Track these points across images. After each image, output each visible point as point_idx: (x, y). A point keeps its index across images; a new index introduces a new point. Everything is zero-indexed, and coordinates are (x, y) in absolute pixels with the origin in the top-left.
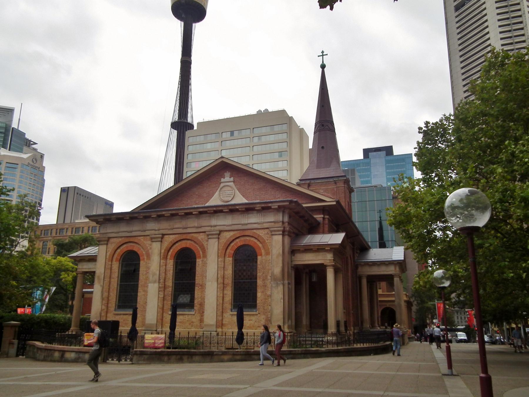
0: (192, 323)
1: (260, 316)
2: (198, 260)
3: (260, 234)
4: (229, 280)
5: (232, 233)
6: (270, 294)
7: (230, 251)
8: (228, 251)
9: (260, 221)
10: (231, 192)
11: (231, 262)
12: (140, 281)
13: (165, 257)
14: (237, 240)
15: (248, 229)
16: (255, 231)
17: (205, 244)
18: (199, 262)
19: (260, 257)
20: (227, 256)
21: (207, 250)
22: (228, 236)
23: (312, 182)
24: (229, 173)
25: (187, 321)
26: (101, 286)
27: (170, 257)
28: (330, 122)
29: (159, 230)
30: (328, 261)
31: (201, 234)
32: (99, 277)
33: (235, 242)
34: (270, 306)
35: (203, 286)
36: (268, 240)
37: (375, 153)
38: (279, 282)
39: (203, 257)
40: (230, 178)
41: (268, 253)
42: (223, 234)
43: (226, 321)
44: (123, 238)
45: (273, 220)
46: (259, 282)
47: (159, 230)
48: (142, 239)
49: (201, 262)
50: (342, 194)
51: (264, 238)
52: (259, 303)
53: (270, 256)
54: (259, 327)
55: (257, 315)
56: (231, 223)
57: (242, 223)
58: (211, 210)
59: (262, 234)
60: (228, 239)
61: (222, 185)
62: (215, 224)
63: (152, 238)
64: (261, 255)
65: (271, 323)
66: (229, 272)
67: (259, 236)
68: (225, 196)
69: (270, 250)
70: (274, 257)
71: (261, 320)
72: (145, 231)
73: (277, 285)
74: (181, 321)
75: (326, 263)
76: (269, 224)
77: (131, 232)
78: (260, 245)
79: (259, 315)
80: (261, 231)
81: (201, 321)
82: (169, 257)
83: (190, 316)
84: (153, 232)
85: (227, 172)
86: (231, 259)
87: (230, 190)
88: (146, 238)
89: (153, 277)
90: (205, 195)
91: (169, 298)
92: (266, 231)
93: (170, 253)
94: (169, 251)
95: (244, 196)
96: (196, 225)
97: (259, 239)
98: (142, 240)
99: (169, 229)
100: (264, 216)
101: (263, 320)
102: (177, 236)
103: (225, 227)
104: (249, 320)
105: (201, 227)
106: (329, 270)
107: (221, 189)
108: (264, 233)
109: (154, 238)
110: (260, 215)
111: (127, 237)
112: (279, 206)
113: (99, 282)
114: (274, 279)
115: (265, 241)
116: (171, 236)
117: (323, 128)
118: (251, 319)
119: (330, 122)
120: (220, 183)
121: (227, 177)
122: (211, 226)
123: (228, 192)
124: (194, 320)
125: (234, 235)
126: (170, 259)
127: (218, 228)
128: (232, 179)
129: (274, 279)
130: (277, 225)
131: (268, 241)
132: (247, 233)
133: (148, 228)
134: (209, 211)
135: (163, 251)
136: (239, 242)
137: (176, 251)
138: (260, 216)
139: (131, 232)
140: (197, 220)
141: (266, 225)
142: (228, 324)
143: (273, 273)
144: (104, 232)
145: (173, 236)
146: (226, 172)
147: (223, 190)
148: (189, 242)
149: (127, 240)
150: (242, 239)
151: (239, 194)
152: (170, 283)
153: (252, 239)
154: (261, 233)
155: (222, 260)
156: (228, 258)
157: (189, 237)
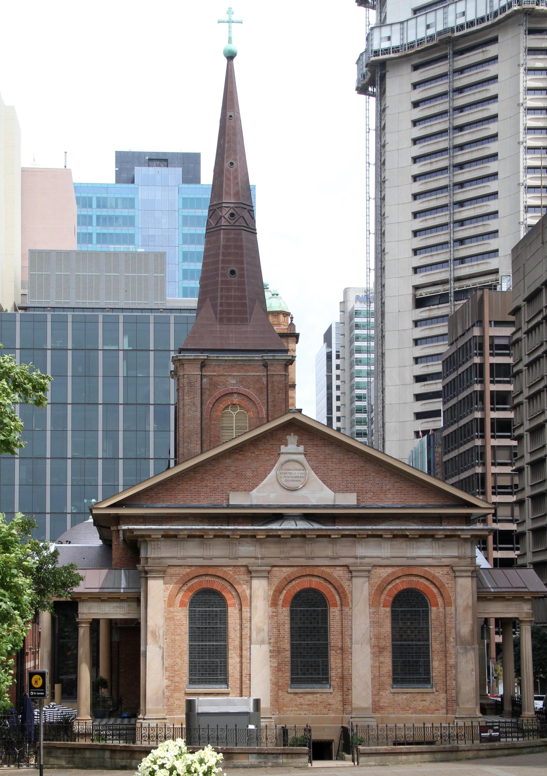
0: (329, 706)
1: (437, 695)
2: (332, 609)
3: (436, 574)
4: (388, 643)
5: (390, 570)
6: (454, 663)
7: (387, 597)
8: (383, 597)
9: (437, 554)
10: (300, 472)
11: (389, 614)
12: (230, 641)
13: (274, 603)
14: (398, 581)
15: (416, 566)
16: (427, 568)
17: (345, 584)
18: (334, 613)
19: (436, 608)
20: (382, 605)
21: (349, 595)
22: (384, 573)
23: (213, 356)
24: (296, 438)
25: (321, 702)
26: (160, 647)
27: (283, 602)
28: (249, 208)
29: (262, 558)
30: (524, 615)
31: (338, 568)
32: (154, 633)
33: (394, 584)
34: (454, 680)
35: (344, 651)
36: (448, 584)
37: (152, 170)
38: (468, 647)
39: (341, 605)
40: (298, 446)
41: (447, 603)
42: (376, 570)
43: (384, 702)
44: (193, 568)
45: (456, 554)
46: (435, 646)
47: (262, 558)
48: (231, 571)
49: (337, 613)
50: (279, 393)
51: (444, 581)
52: (436, 676)
53: (453, 608)
54: (437, 710)
55: (433, 693)
56: (389, 555)
57: (408, 555)
58: (362, 535)
59: (440, 574)
60: (384, 579)
61: (283, 458)
62: (363, 555)
63: (250, 572)
64: (437, 605)
65: (458, 705)
66: (387, 628)
67: (434, 577)
68: (291, 479)
69: (452, 599)
70: (460, 610)
71: (440, 701)
72: (237, 558)
73: (466, 651)
74: (309, 703)
75: (522, 617)
76: (451, 559)
77: (211, 559)
78: (435, 591)
79: (436, 693)
80: (439, 570)
81: (346, 702)
82: (280, 602)
83: (325, 696)
84: (252, 560)
85: (292, 434)
86: (388, 609)
87: (300, 470)
88: (237, 569)
89: (257, 635)
90: (249, 474)
91: (287, 667)
92: (446, 569)
93: (282, 597)
94: (281, 593)
95: (324, 481)
96: (330, 554)
97: (434, 581)
98: (231, 573)
99: (281, 558)
100: (443, 546)
101: (443, 700)
102: (295, 569)
103: (379, 559)
104: (421, 701)
105: (338, 558)
106: (525, 628)
107: (282, 465)
108: (441, 572)
109: (256, 571)
110: (437, 544)
111: (202, 566)
112: (472, 536)
113: (156, 642)
114: (462, 642)
115: (444, 585)
116: (284, 569)
117: (232, 222)
118: (424, 699)
119: (249, 208)
120: (279, 454)
121: (292, 443)
122: (356, 557)
123: (296, 472)
124: (331, 701)
125: (393, 573)
126: (283, 606)
127: (367, 560)
128: (301, 449)
129: (462, 642)
130: (463, 562)
131: (450, 585)
132: (415, 571)
133: (241, 554)
134: (359, 535)
135: (271, 593)
136: (401, 585)
137: (293, 594)
138: (437, 546)
139: (211, 559)
140: (331, 545)
141: (446, 561)
142: (387, 706)
143: (457, 634)
144: (156, 556)
145: (289, 569)
146: (290, 435)
147: (285, 467)
148: (315, 579)
149: (202, 571)
150: (405, 579)
151: (316, 477)
152: (287, 646)
153: (422, 580)
154: (439, 573)
155: (375, 610)
156: (382, 608)
157: (316, 571)
